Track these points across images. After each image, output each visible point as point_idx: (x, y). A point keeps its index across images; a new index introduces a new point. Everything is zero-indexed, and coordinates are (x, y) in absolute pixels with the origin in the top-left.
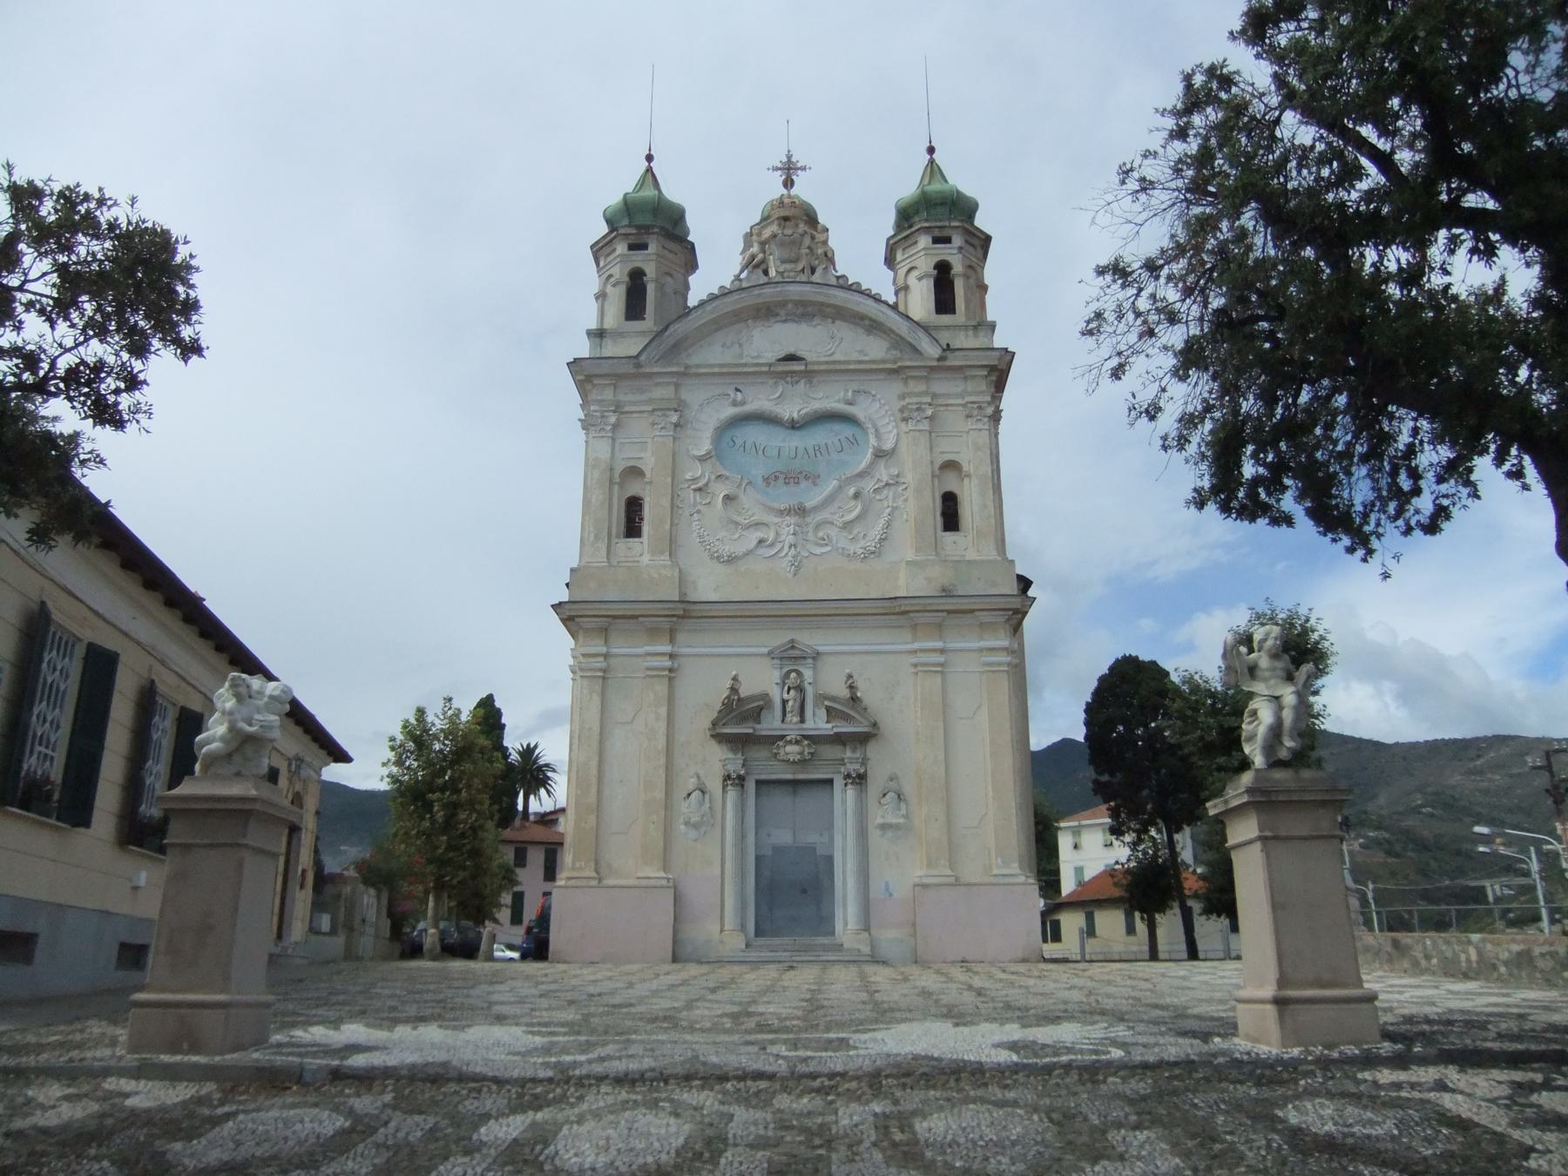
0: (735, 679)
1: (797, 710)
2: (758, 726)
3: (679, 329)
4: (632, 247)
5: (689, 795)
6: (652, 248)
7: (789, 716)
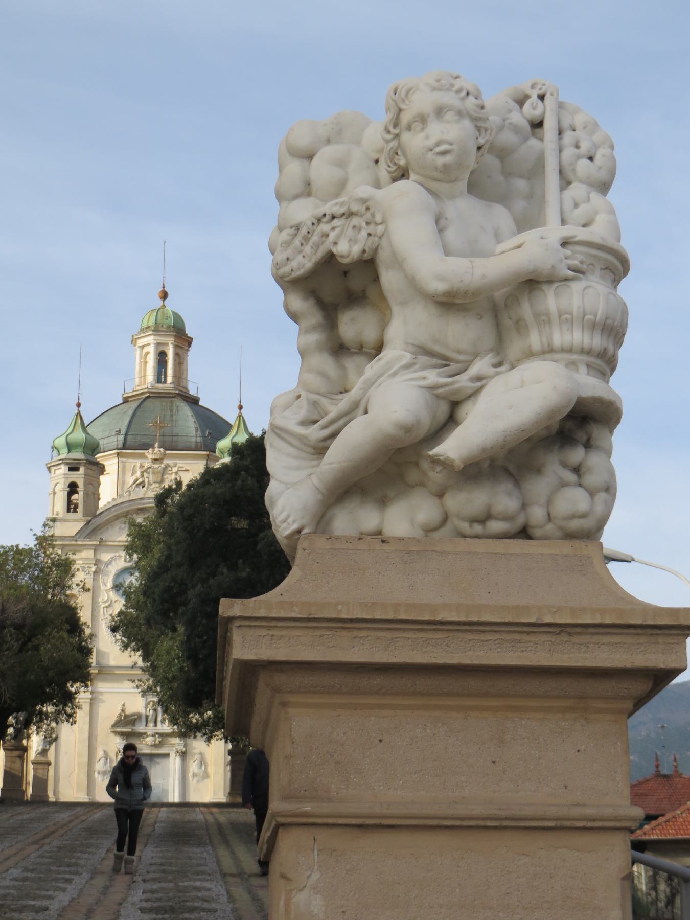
0: (124, 705)
1: (153, 721)
2: (134, 728)
3: (97, 521)
4: (71, 469)
5: (99, 760)
6: (82, 470)
7: (149, 724)
